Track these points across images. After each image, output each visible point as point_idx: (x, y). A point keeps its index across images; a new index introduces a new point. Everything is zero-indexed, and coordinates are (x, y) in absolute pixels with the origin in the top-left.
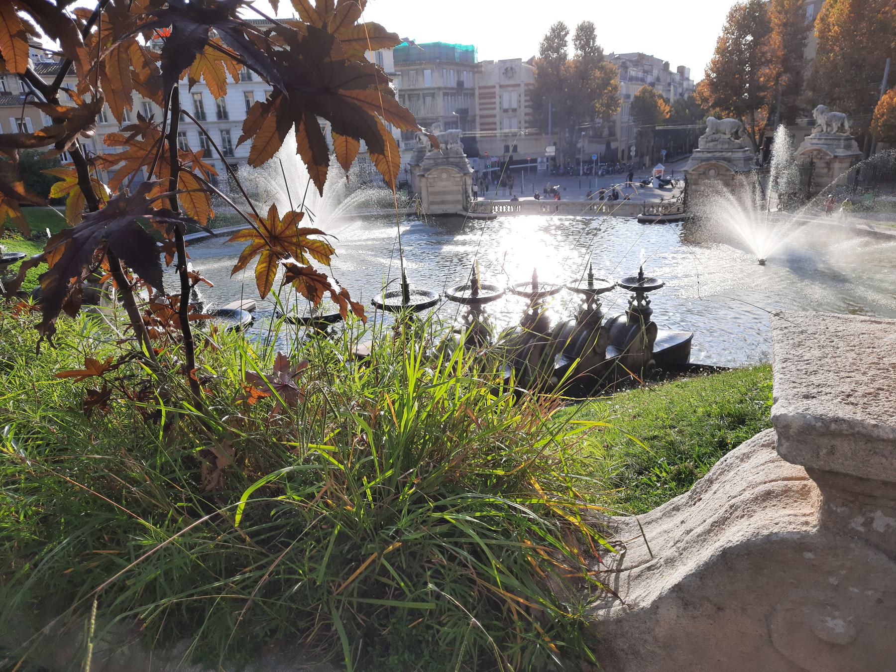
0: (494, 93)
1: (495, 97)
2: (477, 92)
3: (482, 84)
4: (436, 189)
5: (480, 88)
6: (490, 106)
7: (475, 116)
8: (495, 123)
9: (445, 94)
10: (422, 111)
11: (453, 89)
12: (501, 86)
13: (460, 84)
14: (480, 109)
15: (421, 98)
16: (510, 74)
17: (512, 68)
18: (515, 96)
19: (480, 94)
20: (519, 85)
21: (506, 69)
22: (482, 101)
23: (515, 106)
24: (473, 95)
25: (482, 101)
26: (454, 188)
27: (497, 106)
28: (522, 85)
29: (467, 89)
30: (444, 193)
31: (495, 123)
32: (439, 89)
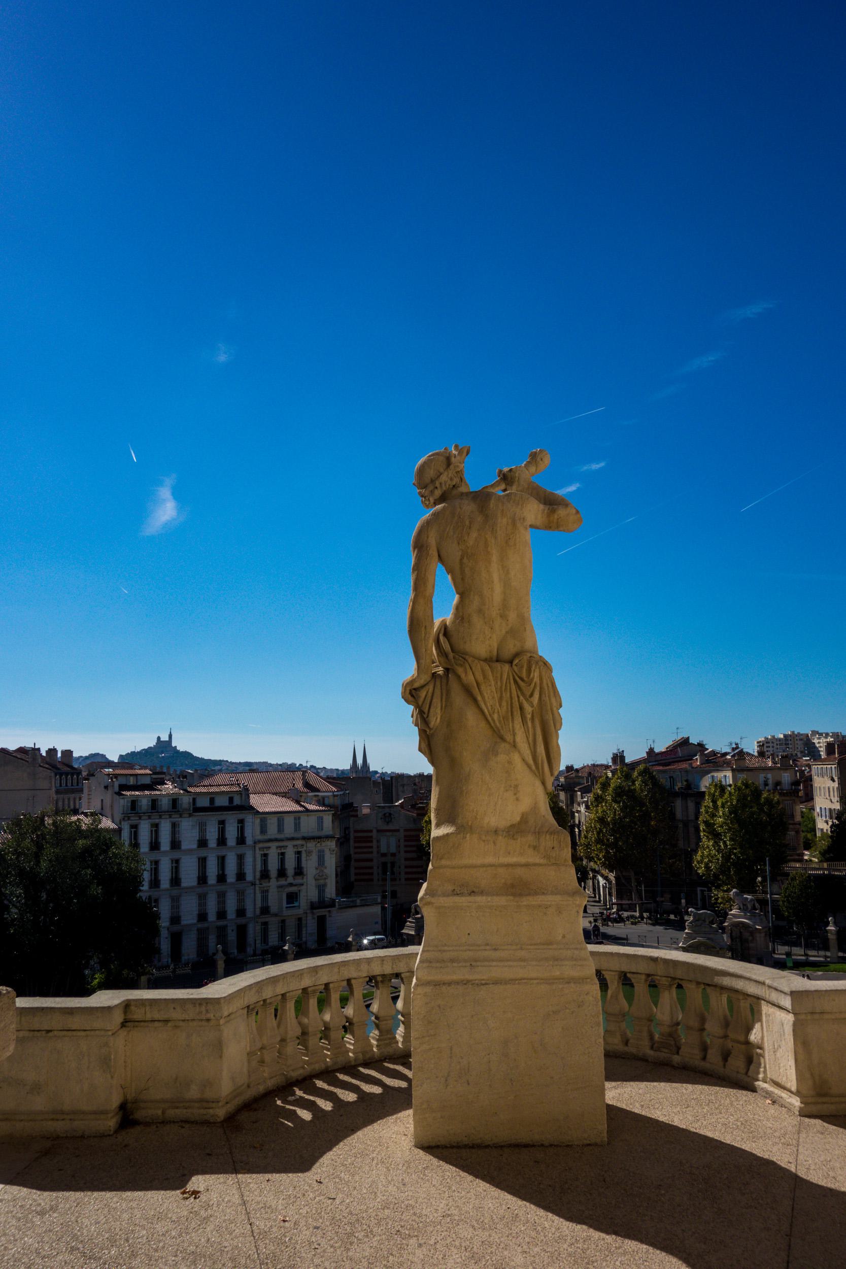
0: (371, 837)
1: (372, 842)
5: (356, 831)
6: (365, 850)
8: (372, 868)
12: (378, 831)
17: (390, 814)
18: (393, 841)
19: (355, 837)
20: (398, 831)
22: (357, 845)
23: (393, 850)
25: (357, 845)
27: (375, 850)
28: (402, 831)
31: (372, 868)
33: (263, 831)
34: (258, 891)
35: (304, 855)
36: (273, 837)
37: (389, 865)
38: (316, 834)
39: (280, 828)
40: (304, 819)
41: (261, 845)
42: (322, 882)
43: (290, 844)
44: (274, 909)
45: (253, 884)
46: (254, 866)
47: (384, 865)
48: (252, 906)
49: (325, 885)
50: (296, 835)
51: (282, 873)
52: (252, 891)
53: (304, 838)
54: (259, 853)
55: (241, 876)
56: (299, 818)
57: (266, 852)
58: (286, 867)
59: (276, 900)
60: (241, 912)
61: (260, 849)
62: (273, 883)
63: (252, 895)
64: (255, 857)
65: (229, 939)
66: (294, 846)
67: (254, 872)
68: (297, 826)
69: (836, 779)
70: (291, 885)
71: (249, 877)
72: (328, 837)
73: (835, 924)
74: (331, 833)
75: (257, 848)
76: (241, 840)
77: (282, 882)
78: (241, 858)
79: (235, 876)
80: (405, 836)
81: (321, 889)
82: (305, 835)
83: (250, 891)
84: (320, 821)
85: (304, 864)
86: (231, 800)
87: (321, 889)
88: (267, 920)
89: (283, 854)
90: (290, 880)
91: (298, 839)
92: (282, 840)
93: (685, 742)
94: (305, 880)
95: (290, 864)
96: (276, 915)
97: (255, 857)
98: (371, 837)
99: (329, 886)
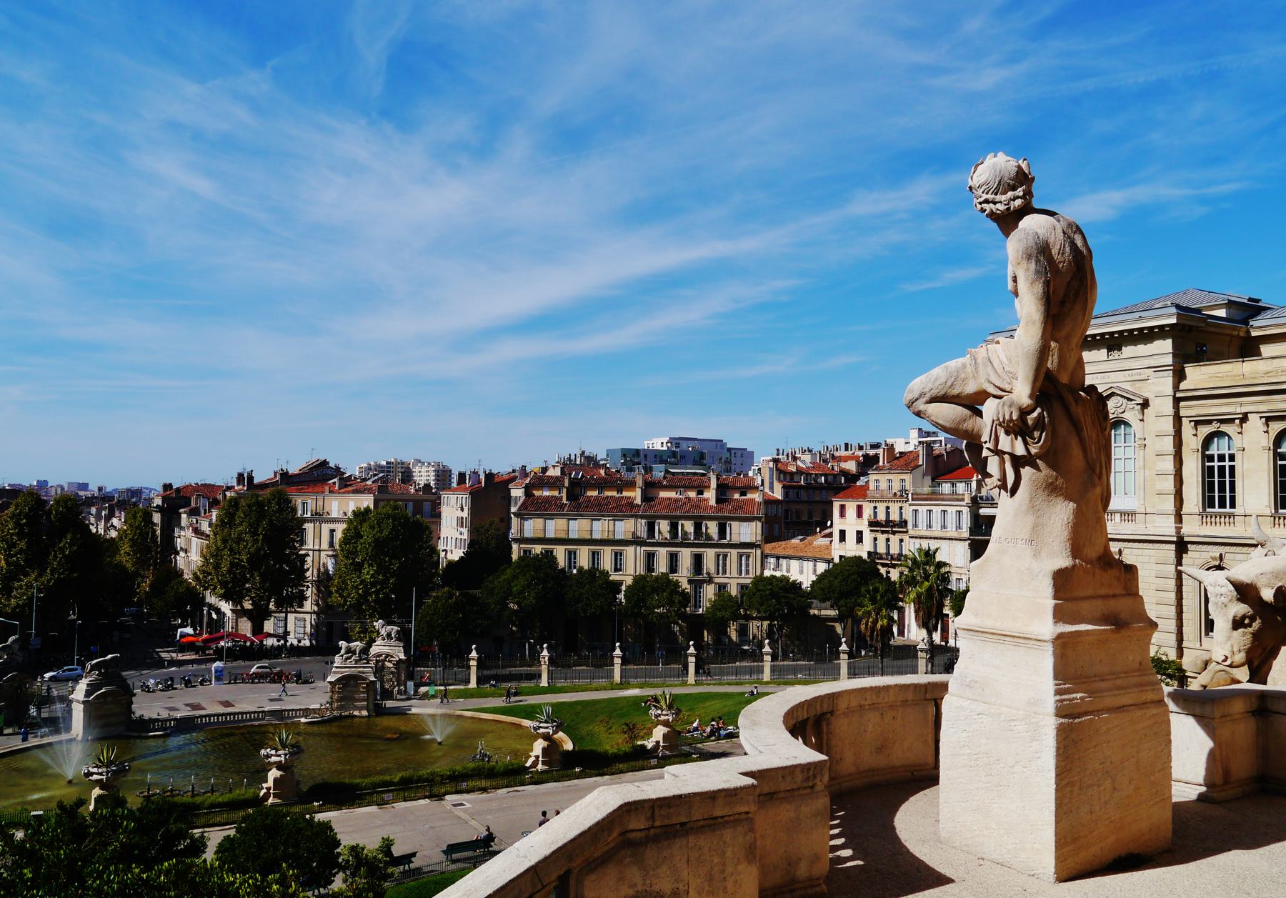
69: (466, 509)
93: (325, 463)
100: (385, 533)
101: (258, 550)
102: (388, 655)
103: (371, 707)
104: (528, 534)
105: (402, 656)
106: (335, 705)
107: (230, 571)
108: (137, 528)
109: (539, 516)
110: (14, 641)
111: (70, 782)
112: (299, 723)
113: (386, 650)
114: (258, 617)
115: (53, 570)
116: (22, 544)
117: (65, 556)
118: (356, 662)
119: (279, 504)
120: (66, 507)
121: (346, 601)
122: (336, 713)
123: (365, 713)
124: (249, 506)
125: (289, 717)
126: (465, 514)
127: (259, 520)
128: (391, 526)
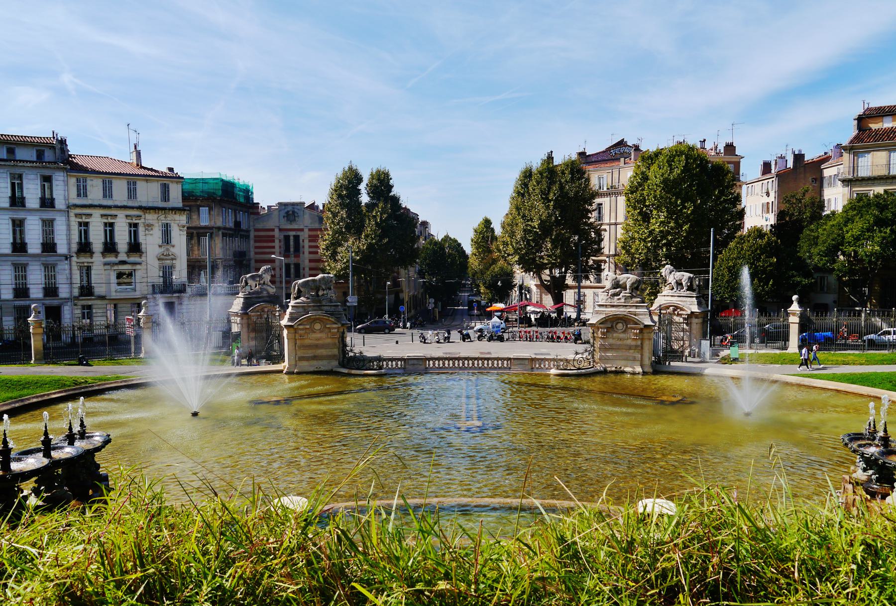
0: (273, 236)
1: (273, 241)
2: (252, 234)
3: (260, 226)
4: (307, 342)
5: (256, 230)
7: (250, 260)
9: (224, 235)
10: (196, 252)
11: (230, 229)
13: (237, 224)
14: (256, 253)
15: (196, 238)
16: (292, 218)
17: (294, 212)
19: (255, 236)
20: (302, 230)
21: (287, 212)
24: (248, 237)
26: (329, 341)
28: (306, 230)
29: (243, 231)
30: (317, 346)
32: (219, 228)
33: (82, 191)
34: (75, 268)
35: (141, 229)
36: (96, 203)
37: (292, 266)
38: (161, 204)
39: (107, 192)
40: (141, 186)
41: (78, 211)
42: (168, 262)
43: (121, 214)
44: (99, 290)
45: (67, 257)
46: (69, 235)
47: (288, 266)
48: (67, 282)
49: (172, 267)
50: (130, 204)
51: (110, 247)
52: (67, 267)
53: (140, 208)
54: (74, 222)
55: (49, 247)
56: (135, 184)
57: (84, 219)
58: (116, 240)
59: (103, 278)
60: (51, 291)
61: (76, 215)
62: (97, 260)
63: (67, 272)
64: (69, 226)
65: (11, 318)
66: (127, 216)
67: (69, 244)
68: (132, 193)
69: (772, 194)
70: (123, 263)
71: (62, 249)
72: (174, 210)
73: (800, 302)
74: (180, 205)
75: (72, 214)
76: (47, 203)
77: (111, 259)
78: (48, 225)
79: (40, 246)
80: (310, 236)
81: (167, 272)
82: (144, 205)
83: (63, 266)
84: (165, 190)
85: (142, 239)
86: (40, 155)
87: (167, 272)
88: (90, 303)
89: (112, 225)
90: (122, 257)
91: (132, 208)
92: (109, 207)
93: (621, 143)
94: (143, 259)
95: (122, 238)
96: (102, 298)
97: (69, 226)
98: (273, 236)
99: (178, 268)
100: (677, 172)
101: (550, 216)
102: (676, 308)
103: (647, 362)
104: (863, 173)
105: (695, 309)
106: (597, 356)
107: (524, 238)
108: (480, 233)
109: (878, 148)
110: (266, 271)
111: (195, 414)
112: (549, 375)
113: (675, 300)
114: (556, 288)
115: (367, 236)
116: (344, 213)
117: (376, 223)
118: (626, 298)
119: (572, 173)
120: (379, 179)
121: (633, 258)
122: (599, 367)
123: (639, 369)
124: (541, 173)
125: (540, 368)
126: (772, 198)
127: (549, 188)
128: (683, 163)
